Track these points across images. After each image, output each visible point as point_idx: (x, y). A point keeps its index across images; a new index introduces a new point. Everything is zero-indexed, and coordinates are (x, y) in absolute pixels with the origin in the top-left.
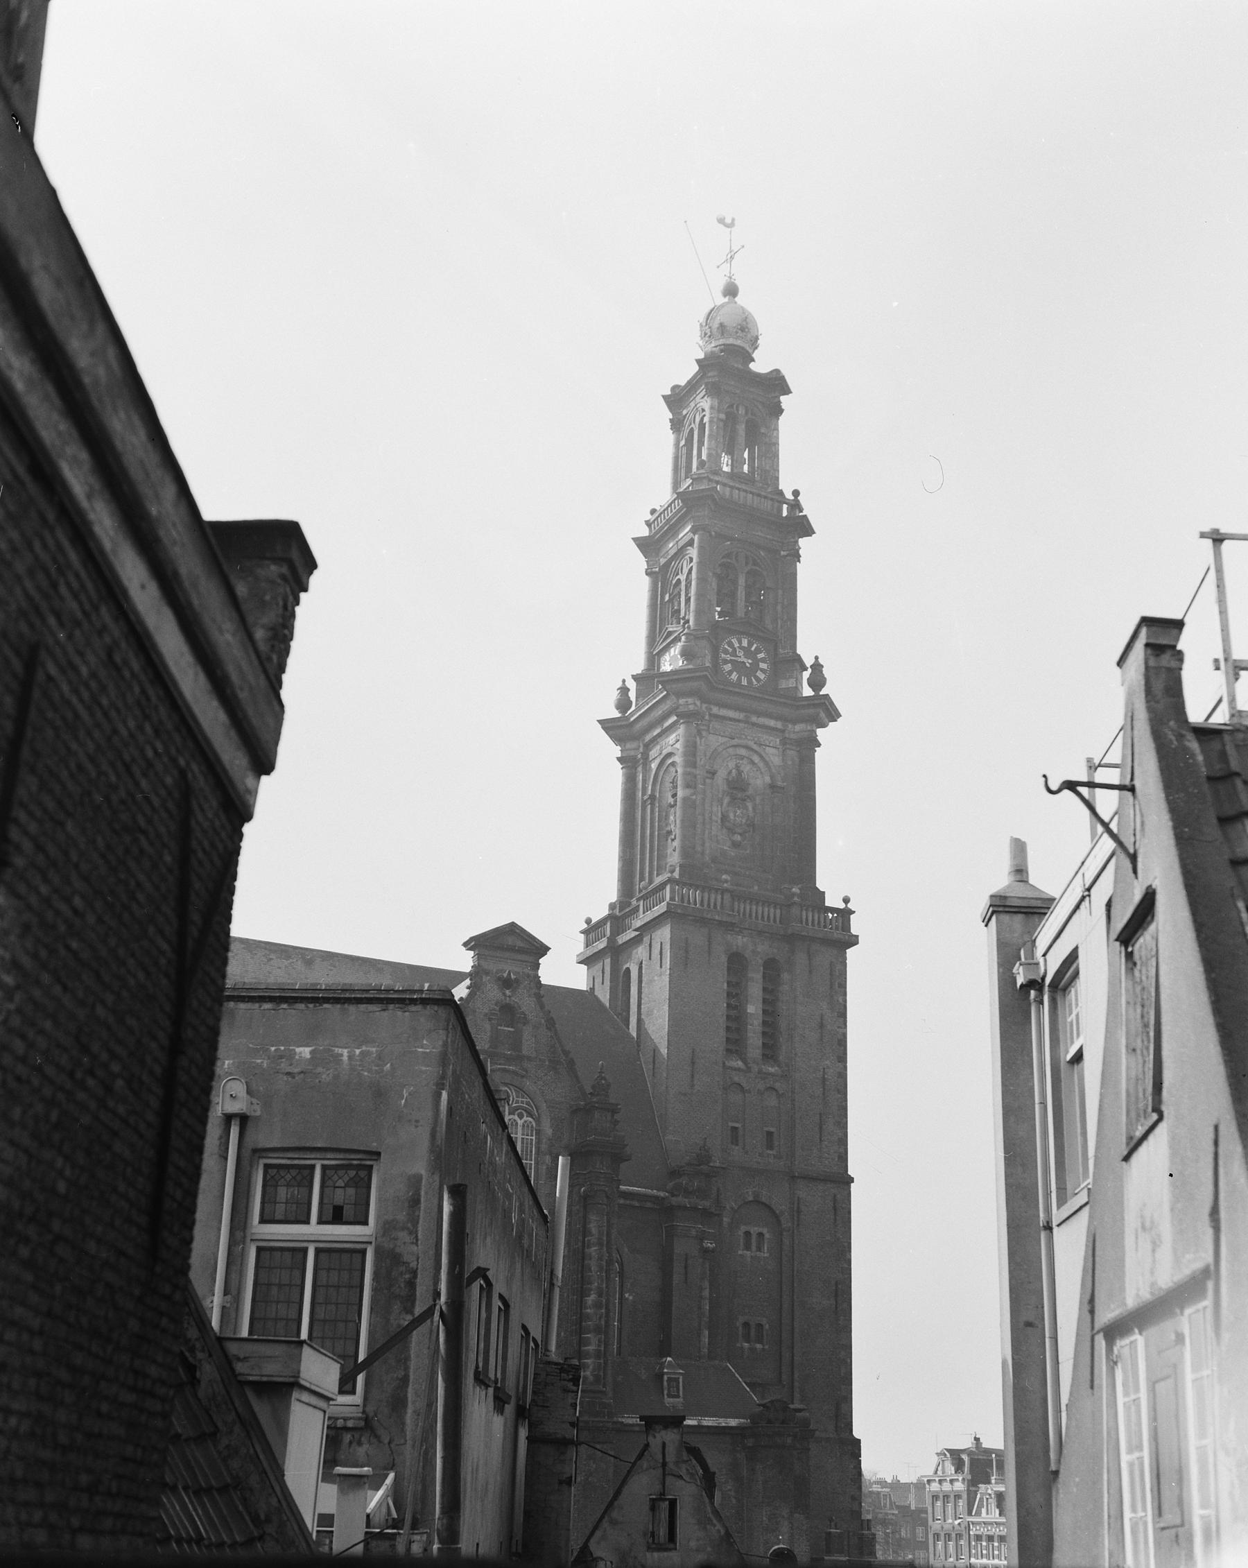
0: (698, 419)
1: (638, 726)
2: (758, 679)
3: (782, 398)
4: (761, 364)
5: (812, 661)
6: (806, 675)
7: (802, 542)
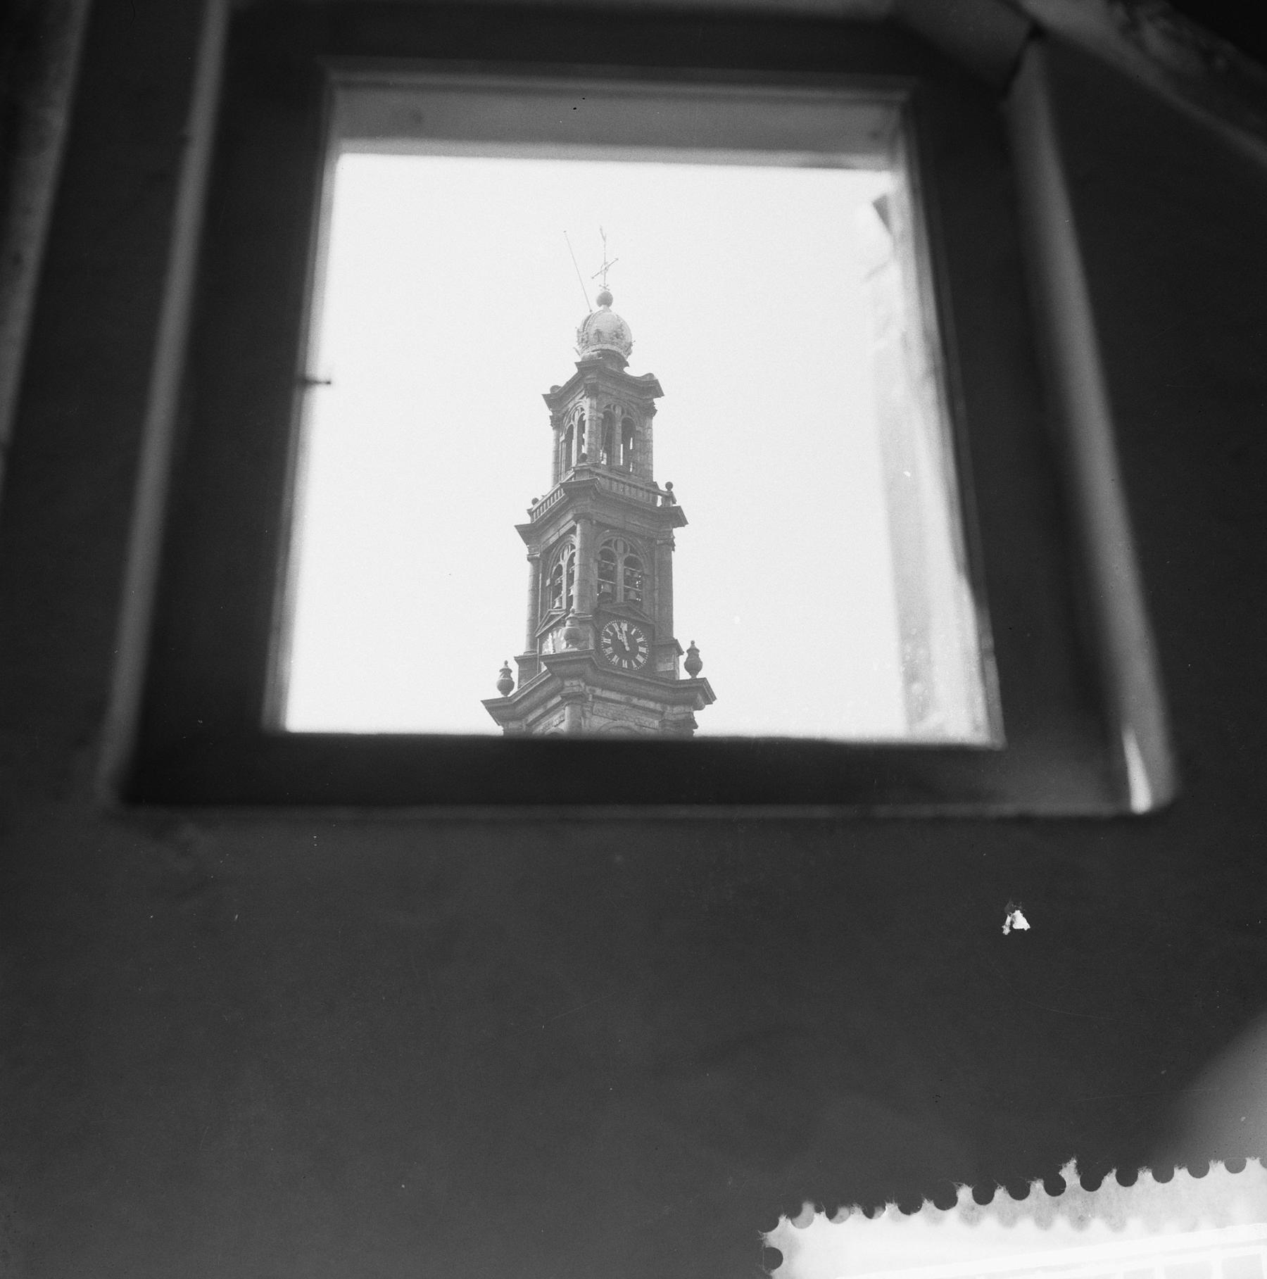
0: (577, 418)
1: (520, 708)
2: (638, 663)
3: (655, 400)
4: (635, 368)
5: (689, 646)
6: (683, 659)
7: (677, 532)
